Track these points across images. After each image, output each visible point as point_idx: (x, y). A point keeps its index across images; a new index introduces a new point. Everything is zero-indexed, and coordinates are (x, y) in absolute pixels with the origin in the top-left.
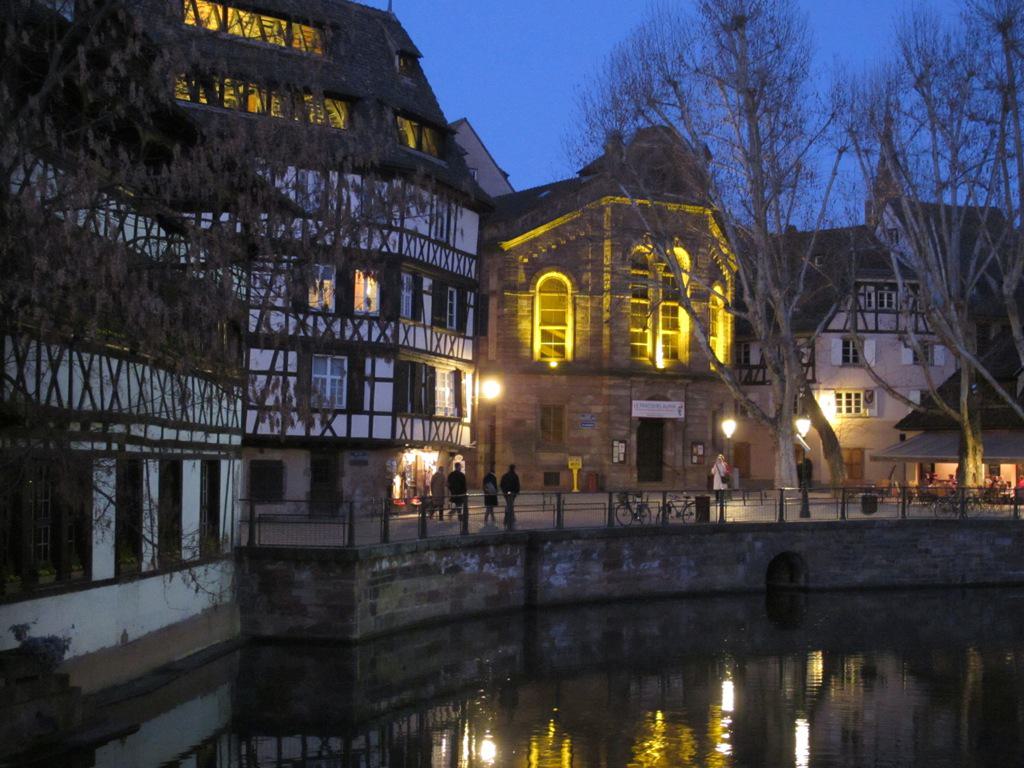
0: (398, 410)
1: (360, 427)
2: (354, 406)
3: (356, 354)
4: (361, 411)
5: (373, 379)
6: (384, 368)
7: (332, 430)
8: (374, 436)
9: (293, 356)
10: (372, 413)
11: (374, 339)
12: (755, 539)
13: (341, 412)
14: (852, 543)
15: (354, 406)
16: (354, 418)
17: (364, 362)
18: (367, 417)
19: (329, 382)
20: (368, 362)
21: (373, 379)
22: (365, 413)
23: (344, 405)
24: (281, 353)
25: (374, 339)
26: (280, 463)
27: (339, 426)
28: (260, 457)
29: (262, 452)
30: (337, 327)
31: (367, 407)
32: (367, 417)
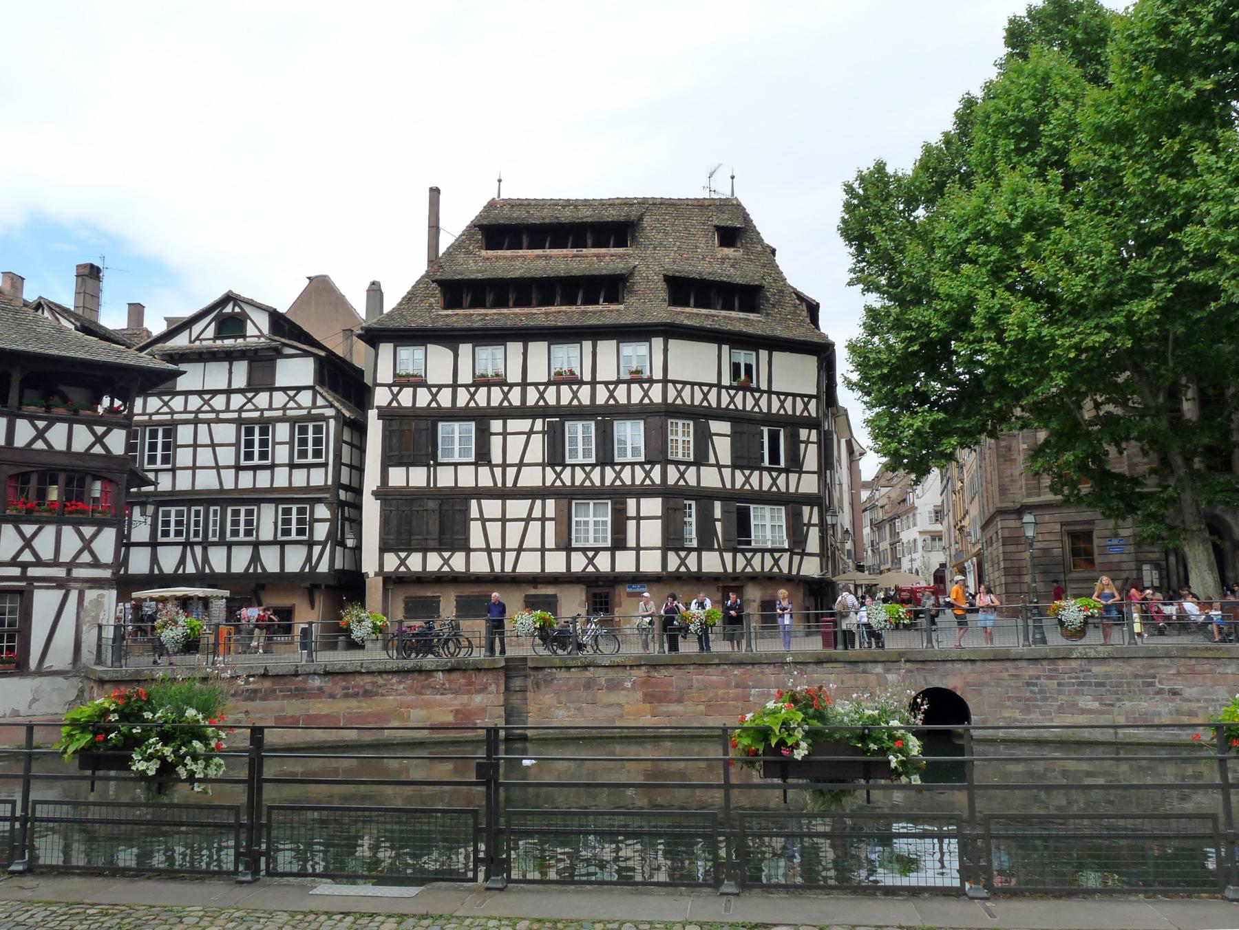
1: (625, 562)
2: (619, 544)
3: (618, 496)
4: (625, 548)
5: (638, 518)
6: (653, 506)
10: (638, 549)
11: (638, 482)
12: (888, 671)
14: (1038, 678)
15: (619, 544)
17: (625, 503)
20: (631, 503)
21: (638, 518)
23: (609, 544)
26: (555, 596)
27: (603, 563)
28: (533, 592)
29: (535, 588)
31: (631, 542)
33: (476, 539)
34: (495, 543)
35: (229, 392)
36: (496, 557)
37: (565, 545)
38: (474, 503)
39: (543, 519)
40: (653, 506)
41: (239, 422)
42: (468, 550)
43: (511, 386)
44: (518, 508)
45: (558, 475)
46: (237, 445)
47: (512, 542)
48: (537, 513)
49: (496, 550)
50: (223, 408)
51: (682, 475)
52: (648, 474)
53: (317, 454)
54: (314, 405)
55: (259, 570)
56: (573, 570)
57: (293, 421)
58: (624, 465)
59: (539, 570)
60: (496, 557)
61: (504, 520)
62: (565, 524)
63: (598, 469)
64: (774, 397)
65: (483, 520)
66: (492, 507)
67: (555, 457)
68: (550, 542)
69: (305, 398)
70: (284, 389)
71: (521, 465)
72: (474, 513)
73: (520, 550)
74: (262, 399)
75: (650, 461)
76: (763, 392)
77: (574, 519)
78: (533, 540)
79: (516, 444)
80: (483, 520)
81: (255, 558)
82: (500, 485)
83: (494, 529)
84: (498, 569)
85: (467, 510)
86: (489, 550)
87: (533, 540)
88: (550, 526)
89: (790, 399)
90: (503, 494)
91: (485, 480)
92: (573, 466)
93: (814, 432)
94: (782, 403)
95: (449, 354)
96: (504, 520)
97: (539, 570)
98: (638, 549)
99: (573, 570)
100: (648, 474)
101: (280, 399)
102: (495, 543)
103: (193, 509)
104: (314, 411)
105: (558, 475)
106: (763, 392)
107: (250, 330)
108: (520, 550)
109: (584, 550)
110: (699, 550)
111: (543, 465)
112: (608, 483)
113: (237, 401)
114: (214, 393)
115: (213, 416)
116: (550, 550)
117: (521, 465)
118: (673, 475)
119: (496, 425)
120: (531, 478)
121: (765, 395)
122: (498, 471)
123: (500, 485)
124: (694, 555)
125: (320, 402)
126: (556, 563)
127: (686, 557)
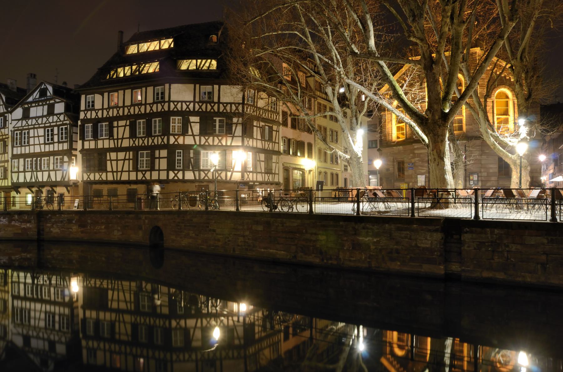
0: (168, 170)
1: (155, 175)
2: (152, 169)
5: (159, 158)
6: (164, 153)
7: (145, 177)
8: (160, 178)
9: (131, 153)
10: (159, 170)
13: (148, 170)
15: (152, 169)
16: (153, 172)
18: (157, 172)
19: (145, 161)
22: (157, 170)
24: (128, 153)
25: (159, 143)
26: (136, 189)
28: (130, 187)
29: (130, 186)
30: (146, 142)
31: (157, 167)
32: (157, 172)
33: (109, 169)
34: (115, 169)
35: (43, 117)
36: (115, 174)
37: (136, 169)
38: (108, 154)
39: (129, 159)
40: (164, 153)
41: (45, 128)
42: (107, 172)
43: (120, 107)
44: (121, 155)
45: (134, 142)
46: (44, 136)
47: (120, 169)
48: (127, 157)
49: (115, 172)
50: (52, 121)
51: (176, 140)
52: (163, 140)
53: (66, 138)
54: (64, 120)
55: (50, 180)
56: (96, 179)
57: (58, 126)
58: (155, 136)
59: (128, 179)
60: (115, 174)
61: (117, 160)
62: (136, 160)
63: (147, 139)
64: (221, 105)
65: (111, 160)
66: (113, 155)
67: (133, 135)
68: (131, 169)
69: (62, 117)
70: (56, 115)
71: (123, 138)
72: (108, 158)
73: (122, 171)
74: (51, 119)
75: (164, 135)
76: (215, 103)
77: (139, 159)
78: (126, 168)
79: (121, 130)
80: (111, 160)
81: (49, 176)
82: (116, 147)
83: (114, 163)
84: (115, 179)
85: (106, 156)
86: (113, 172)
87: (126, 168)
88: (131, 161)
89: (229, 105)
90: (117, 150)
91: (112, 146)
92: (139, 138)
93: (241, 119)
94: (225, 107)
95: (101, 97)
96: (117, 160)
97: (128, 179)
98: (159, 170)
99: (96, 179)
100: (163, 140)
101: (55, 118)
102: (115, 169)
103: (55, 157)
104: (64, 122)
105: (134, 142)
106: (215, 103)
107: (48, 94)
108: (122, 171)
109: (142, 171)
110: (183, 171)
111: (129, 138)
112: (150, 144)
113: (45, 119)
114: (39, 117)
115: (38, 126)
116: (131, 171)
117: (123, 138)
118: (172, 140)
119: (115, 124)
120: (126, 143)
121: (216, 105)
122: (116, 141)
123: (116, 147)
124: (181, 173)
125: (66, 119)
126: (133, 176)
127: (178, 173)
